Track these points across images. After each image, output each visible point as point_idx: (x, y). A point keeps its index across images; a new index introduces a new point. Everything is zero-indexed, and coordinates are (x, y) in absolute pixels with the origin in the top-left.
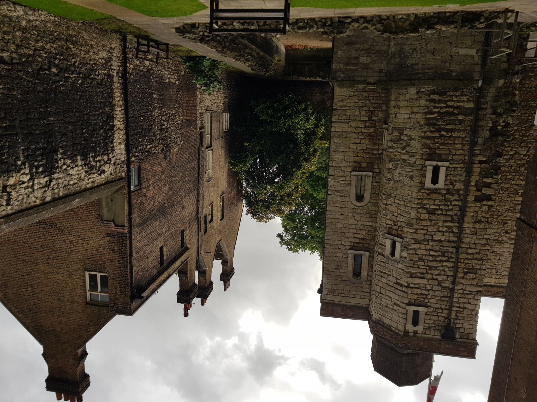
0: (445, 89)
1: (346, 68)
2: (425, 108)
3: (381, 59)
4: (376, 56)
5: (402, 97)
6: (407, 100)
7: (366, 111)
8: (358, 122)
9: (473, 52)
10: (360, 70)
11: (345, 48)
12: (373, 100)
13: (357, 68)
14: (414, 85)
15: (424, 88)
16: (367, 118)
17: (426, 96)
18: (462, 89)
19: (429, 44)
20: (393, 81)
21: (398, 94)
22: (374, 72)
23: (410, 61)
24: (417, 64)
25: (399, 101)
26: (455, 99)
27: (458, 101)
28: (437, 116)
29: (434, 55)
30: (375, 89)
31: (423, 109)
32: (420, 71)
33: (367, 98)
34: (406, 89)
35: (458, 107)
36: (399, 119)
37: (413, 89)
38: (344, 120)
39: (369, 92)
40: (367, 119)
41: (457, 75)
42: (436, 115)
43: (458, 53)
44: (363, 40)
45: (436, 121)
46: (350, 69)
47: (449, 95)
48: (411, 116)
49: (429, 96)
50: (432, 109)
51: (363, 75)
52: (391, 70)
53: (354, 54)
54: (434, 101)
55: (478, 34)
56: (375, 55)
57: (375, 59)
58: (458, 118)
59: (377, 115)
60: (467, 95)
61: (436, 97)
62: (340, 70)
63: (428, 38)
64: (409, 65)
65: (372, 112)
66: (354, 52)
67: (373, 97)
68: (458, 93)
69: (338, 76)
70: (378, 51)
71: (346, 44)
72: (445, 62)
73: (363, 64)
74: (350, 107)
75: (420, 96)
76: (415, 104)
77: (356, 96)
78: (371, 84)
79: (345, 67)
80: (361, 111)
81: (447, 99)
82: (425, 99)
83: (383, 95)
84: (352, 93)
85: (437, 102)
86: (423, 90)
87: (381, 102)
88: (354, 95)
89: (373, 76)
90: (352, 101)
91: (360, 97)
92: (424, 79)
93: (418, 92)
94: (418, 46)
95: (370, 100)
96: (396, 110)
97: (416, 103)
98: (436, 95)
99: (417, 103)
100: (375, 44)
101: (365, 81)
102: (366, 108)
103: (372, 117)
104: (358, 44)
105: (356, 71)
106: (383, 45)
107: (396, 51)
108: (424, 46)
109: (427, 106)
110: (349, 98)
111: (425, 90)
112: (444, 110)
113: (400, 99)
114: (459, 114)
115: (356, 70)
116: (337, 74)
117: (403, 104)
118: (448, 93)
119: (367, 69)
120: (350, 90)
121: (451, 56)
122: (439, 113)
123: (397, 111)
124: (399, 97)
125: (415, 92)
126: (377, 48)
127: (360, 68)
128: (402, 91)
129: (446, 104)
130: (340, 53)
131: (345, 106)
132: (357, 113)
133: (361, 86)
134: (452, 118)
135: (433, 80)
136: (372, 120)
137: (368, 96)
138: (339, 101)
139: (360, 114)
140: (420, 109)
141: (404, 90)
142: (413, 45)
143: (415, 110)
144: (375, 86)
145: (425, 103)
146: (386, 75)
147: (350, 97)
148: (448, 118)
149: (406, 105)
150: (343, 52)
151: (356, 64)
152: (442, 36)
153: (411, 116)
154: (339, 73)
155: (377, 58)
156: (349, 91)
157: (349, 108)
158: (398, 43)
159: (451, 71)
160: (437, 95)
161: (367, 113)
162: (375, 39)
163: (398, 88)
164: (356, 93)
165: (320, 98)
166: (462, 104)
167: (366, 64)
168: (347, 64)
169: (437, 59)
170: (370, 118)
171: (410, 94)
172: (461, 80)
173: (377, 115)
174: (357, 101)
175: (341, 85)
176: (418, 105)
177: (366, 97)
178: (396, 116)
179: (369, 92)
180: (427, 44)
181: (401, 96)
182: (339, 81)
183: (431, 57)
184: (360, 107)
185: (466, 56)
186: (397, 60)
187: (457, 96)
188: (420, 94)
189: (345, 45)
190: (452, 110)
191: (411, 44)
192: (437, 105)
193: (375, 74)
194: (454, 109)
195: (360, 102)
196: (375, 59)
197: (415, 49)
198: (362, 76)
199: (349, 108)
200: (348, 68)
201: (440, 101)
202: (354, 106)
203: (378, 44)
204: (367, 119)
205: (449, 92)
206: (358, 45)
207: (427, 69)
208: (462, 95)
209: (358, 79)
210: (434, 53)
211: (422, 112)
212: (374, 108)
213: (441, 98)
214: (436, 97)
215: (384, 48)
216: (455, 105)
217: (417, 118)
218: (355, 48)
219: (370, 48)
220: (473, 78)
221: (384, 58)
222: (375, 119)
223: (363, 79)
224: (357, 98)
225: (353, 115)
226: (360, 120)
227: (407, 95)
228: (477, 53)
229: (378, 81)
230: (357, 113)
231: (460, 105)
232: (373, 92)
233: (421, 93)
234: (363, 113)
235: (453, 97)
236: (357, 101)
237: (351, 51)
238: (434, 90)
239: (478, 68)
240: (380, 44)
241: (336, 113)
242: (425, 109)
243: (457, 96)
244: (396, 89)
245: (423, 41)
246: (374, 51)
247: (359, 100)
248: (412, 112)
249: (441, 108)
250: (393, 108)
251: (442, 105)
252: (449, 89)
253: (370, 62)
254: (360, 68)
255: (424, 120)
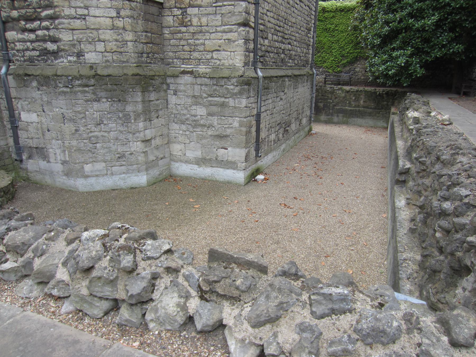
0: (43, 59)
1: (226, 98)
2: (60, 27)
3: (178, 111)
4: (184, 115)
5: (112, 46)
6: (99, 40)
7: (191, 25)
8: (203, 4)
9: (25, 116)
10: (205, 95)
11: (229, 131)
12: (183, 46)
13: (210, 99)
14: (91, 68)
15: (70, 62)
16: (188, 12)
17: (62, 47)
18: (25, 61)
19: (73, 132)
20: (133, 75)
21: (121, 52)
22: (185, 91)
23: (105, 105)
24: (87, 101)
25: (116, 40)
26: (29, 44)
27: (24, 41)
28: (41, 12)
29: (62, 113)
30: (183, 64)
31: (64, 24)
32: (81, 89)
33: (193, 47)
34: (107, 61)
35: (24, 30)
36: (109, 6)
37: (92, 61)
38: (225, 6)
39: (190, 59)
40: (190, 11)
41: (31, 82)
42: (44, 14)
43: (38, 115)
44: (204, 141)
45: (41, 4)
46: (219, 96)
47: (37, 50)
48: (86, 12)
49: (58, 47)
50: (51, 25)
51: (199, 86)
52: (140, 94)
53: (215, 120)
54: (54, 40)
55: (26, 140)
56: (186, 117)
57: (185, 112)
58: (18, 12)
59: (175, 18)
60: (18, 51)
61: (51, 46)
62: (234, 96)
63: (77, 140)
64: (104, 100)
65: (182, 24)
66: (215, 124)
67: (184, 51)
68: (28, 53)
69: (237, 86)
70: (183, 123)
71: (227, 136)
72: (49, 103)
73: (200, 104)
74: (217, 32)
75: (74, 48)
76: (81, 33)
77: (209, 51)
78: (188, 73)
79: (227, 100)
80: (199, 24)
81: (37, 44)
82: (62, 43)
83: (170, 54)
84: (215, 56)
85: (47, 38)
86: (70, 58)
87: (172, 41)
88: (212, 51)
89: (186, 85)
90: (214, 41)
91: (202, 49)
92: (67, 76)
93: (80, 54)
94: (93, 128)
95: (189, 44)
96: (119, 23)
97: (81, 36)
98: (51, 49)
99: (78, 35)
100: (188, 133)
101: (195, 77)
102: (191, 29)
103: (181, 15)
104: (211, 136)
105: (209, 93)
106: (177, 131)
107: (135, 122)
108: (82, 128)
109: (57, 29)
110: (220, 46)
111: (67, 58)
112: (37, 23)
113: (114, 43)
114: (17, 20)
115: (211, 96)
116: (238, 88)
117: (108, 35)
118: (38, 53)
119: (194, 96)
120: (218, 62)
121: (44, 111)
122: (41, 19)
123: (118, 22)
124: (118, 47)
125: (87, 56)
126: (184, 127)
127: (206, 98)
128: (115, 58)
129: (37, 36)
130: (236, 124)
131: (224, 32)
132: (204, 20)
133: (202, 69)
134: (23, 11)
135: (56, 75)
136: (181, 8)
137: (190, 52)
138: (234, 41)
139: (200, 19)
140: (69, 24)
141: (110, 58)
142: (103, 130)
143: (78, 23)
144: (182, 69)
145: (61, 36)
146: (168, 85)
147: (219, 48)
148: (28, 10)
149: (100, 32)
150: (231, 124)
151: (211, 105)
152: (60, 142)
153: (86, 12)
154: (235, 91)
155: (182, 112)
156: (220, 60)
157: (219, 29)
158: (134, 134)
159: (39, 89)
160: (49, 51)
161: (190, 21)
162: (189, 141)
163: (124, 62)
164: (209, 57)
165: (356, 65)
166: (20, 36)
167: (196, 104)
168: (223, 105)
169: (57, 108)
170: (184, 13)
171: (95, 51)
172: (27, 75)
173: (175, 18)
174: (207, 42)
175: (233, 68)
176: (74, 32)
177: (194, 51)
178: (118, 13)
179: (190, 59)
180: (76, 130)
181: (115, 48)
182: (235, 77)
183: (65, 111)
184: (201, 32)
185: (29, 111)
186: (129, 108)
187: (27, 49)
188: (76, 51)
189: (229, 136)
190: (28, 26)
191: (109, 132)
192: (46, 32)
193: (182, 88)
194: (26, 28)
195: (201, 41)
196: (185, 112)
197: (99, 124)
198: (201, 85)
199: (219, 29)
200: (223, 99)
201: (44, 40)
202: (211, 33)
203: (184, 133)
204: (190, 11)
205: (38, 56)
206: (210, 133)
207: (68, 92)
208: (23, 50)
209: (206, 79)
210: (63, 118)
211: (63, 18)
212: (180, 32)
213: (43, 45)
214: (51, 46)
215: (175, 126)
216: (26, 34)
217: (70, 7)
218: (214, 129)
219: (194, 128)
220: (14, 78)
221: (174, 111)
222: (177, 12)
223: (199, 81)
224: (208, 49)
225: (210, 16)
226: (199, 6)
227: (103, 50)
228: (20, 114)
229: (177, 76)
230: (204, 20)
231: (21, 34)
232: (185, 59)
233: (74, 53)
234: (195, 21)
235: (31, 47)
236: (207, 42)
237: (220, 126)
238: (56, 58)
239: (13, 93)
240: (181, 132)
241: (238, 18)
242: (59, 24)
243: (27, 49)
244: (127, 62)
245: (85, 136)
246: (187, 124)
247: (204, 44)
248: (85, 19)
249: (40, 28)
250: (129, 27)
251: (40, 33)
252: (38, 61)
253: (191, 106)
254: (206, 98)
255: (56, 4)
